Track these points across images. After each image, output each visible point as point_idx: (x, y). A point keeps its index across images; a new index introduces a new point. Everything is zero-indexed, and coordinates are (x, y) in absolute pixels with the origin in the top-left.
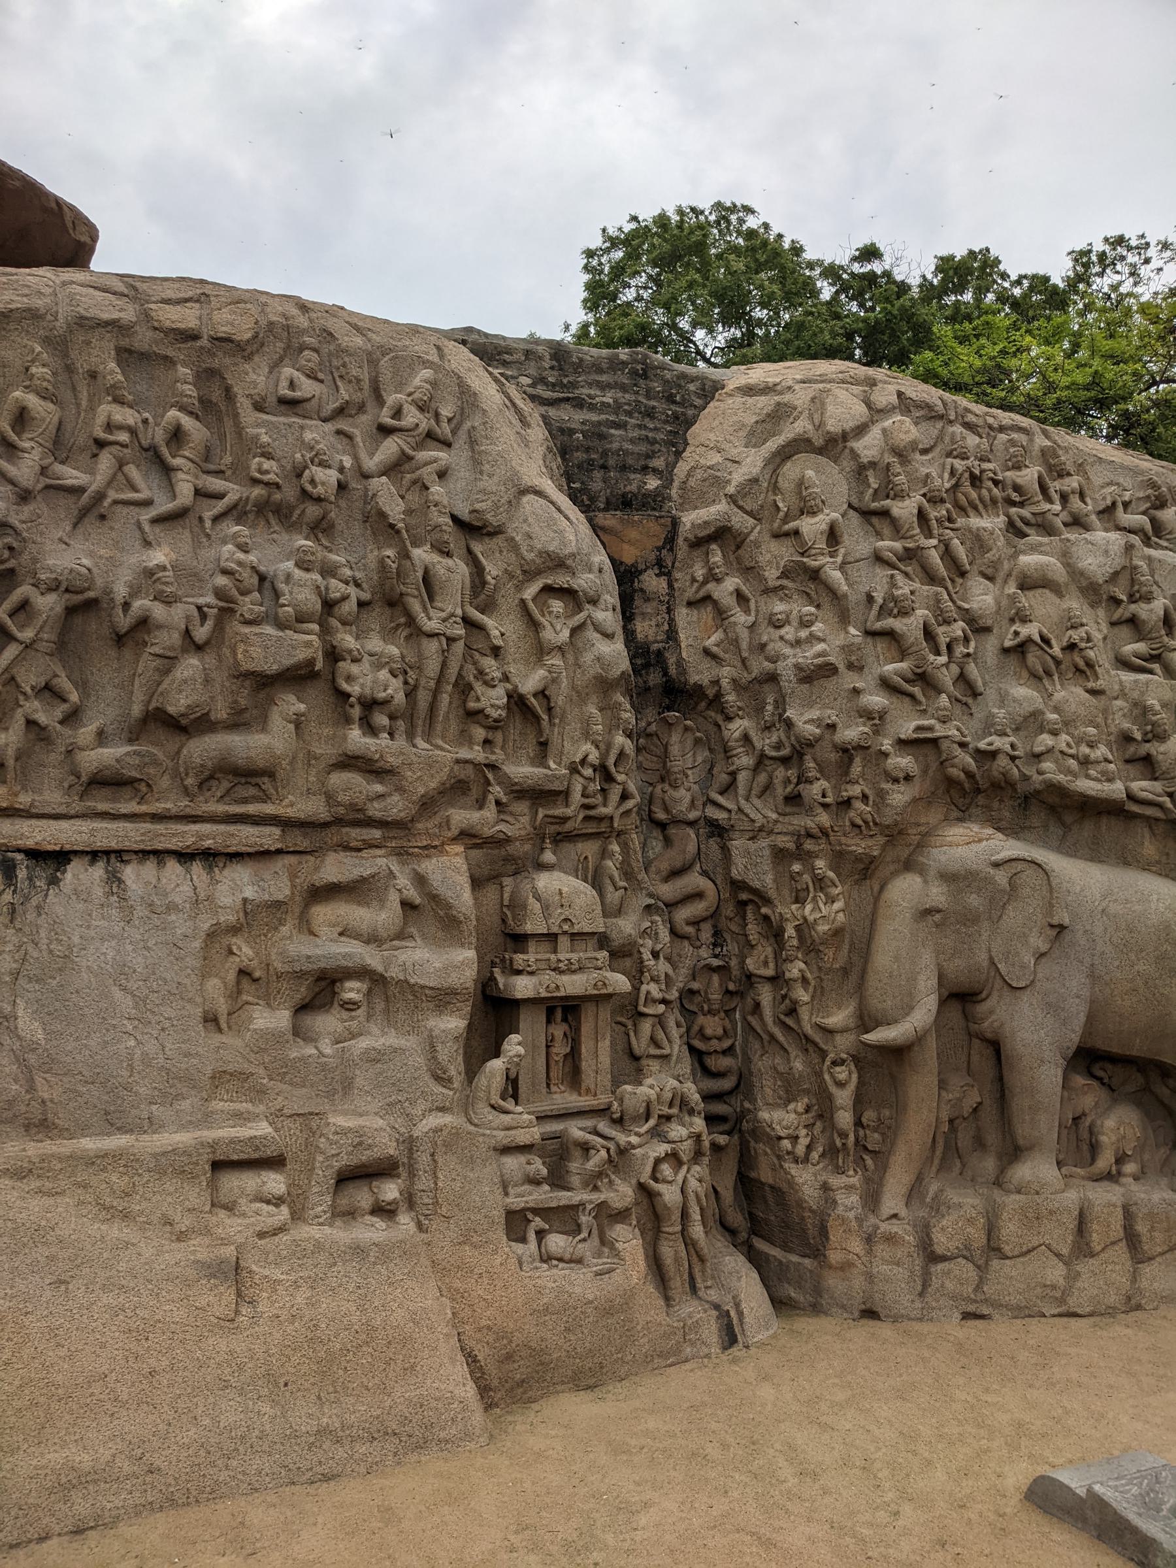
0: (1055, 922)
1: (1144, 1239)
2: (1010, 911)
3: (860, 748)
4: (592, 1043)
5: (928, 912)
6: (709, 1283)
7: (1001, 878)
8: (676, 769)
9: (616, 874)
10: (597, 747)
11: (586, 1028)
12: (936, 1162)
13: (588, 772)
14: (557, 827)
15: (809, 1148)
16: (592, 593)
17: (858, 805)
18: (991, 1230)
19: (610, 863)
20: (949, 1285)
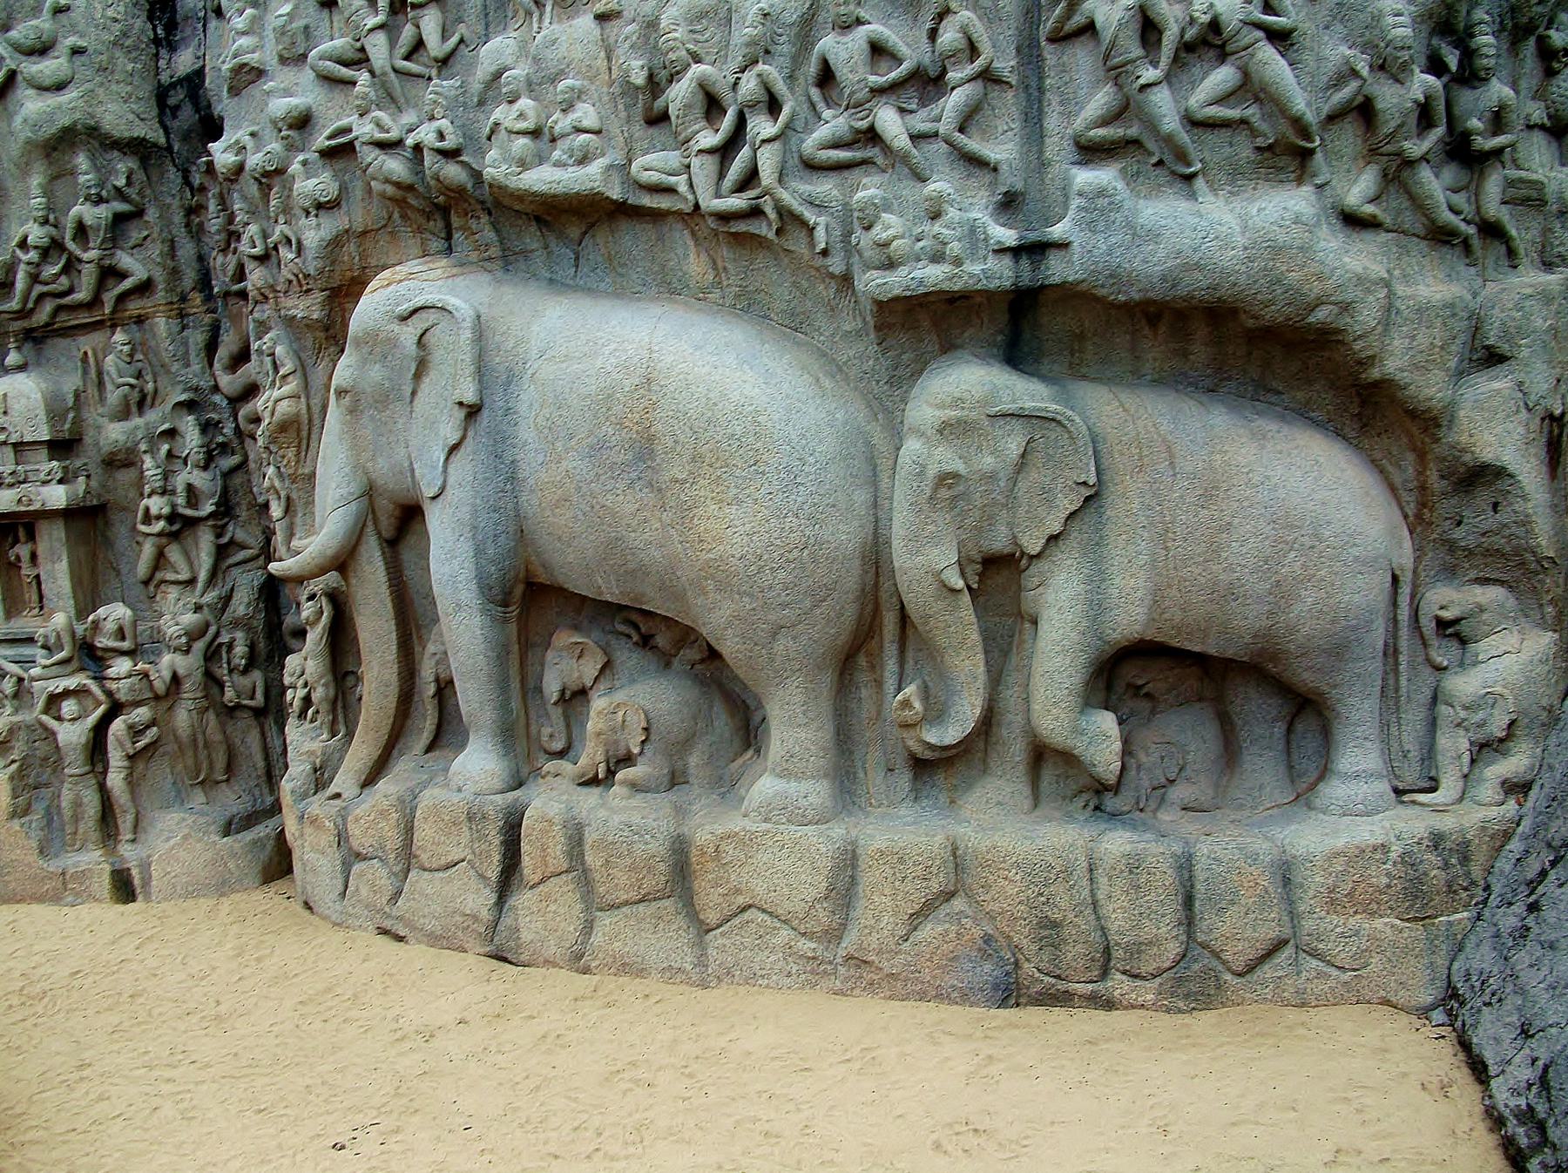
0: (457, 397)
1: (597, 876)
2: (426, 383)
3: (266, 174)
4: (49, 567)
5: (341, 393)
6: (129, 836)
7: (408, 335)
8: (213, 229)
9: (113, 371)
10: (45, 222)
11: (42, 548)
12: (425, 737)
13: (33, 255)
14: (19, 323)
15: (307, 701)
16: (29, 43)
17: (283, 251)
18: (409, 831)
19: (110, 360)
20: (364, 891)
